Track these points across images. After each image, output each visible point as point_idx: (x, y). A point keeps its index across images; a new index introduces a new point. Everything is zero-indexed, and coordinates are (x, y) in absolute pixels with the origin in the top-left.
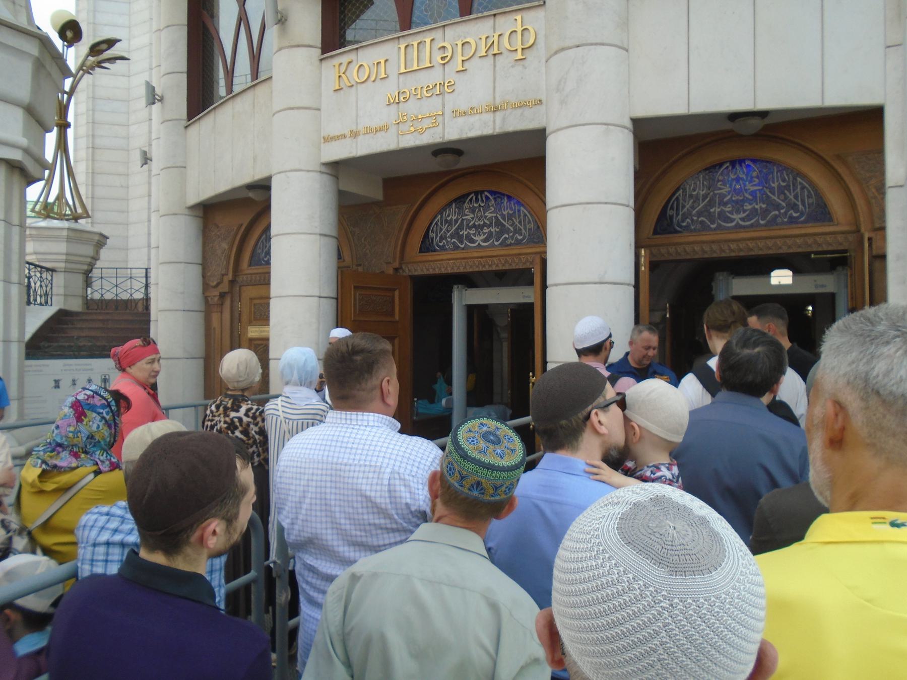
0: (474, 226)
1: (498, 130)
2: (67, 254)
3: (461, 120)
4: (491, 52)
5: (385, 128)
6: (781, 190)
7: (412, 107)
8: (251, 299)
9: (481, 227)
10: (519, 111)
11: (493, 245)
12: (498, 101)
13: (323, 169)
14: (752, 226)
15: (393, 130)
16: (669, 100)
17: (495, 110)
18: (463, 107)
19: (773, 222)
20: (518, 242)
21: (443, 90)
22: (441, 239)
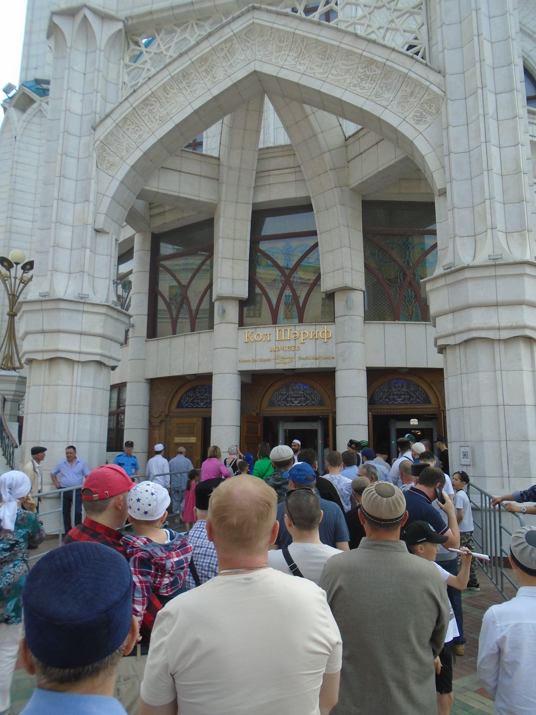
0: (294, 397)
1: (317, 367)
2: (15, 391)
3: (302, 361)
4: (314, 338)
5: (269, 360)
6: (414, 392)
7: (281, 354)
8: (177, 424)
9: (297, 397)
10: (326, 360)
11: (302, 405)
12: (317, 356)
13: (238, 373)
14: (404, 404)
15: (273, 361)
16: (379, 363)
17: (316, 359)
18: (303, 356)
19: (411, 403)
20: (313, 405)
21: (295, 349)
22: (279, 401)
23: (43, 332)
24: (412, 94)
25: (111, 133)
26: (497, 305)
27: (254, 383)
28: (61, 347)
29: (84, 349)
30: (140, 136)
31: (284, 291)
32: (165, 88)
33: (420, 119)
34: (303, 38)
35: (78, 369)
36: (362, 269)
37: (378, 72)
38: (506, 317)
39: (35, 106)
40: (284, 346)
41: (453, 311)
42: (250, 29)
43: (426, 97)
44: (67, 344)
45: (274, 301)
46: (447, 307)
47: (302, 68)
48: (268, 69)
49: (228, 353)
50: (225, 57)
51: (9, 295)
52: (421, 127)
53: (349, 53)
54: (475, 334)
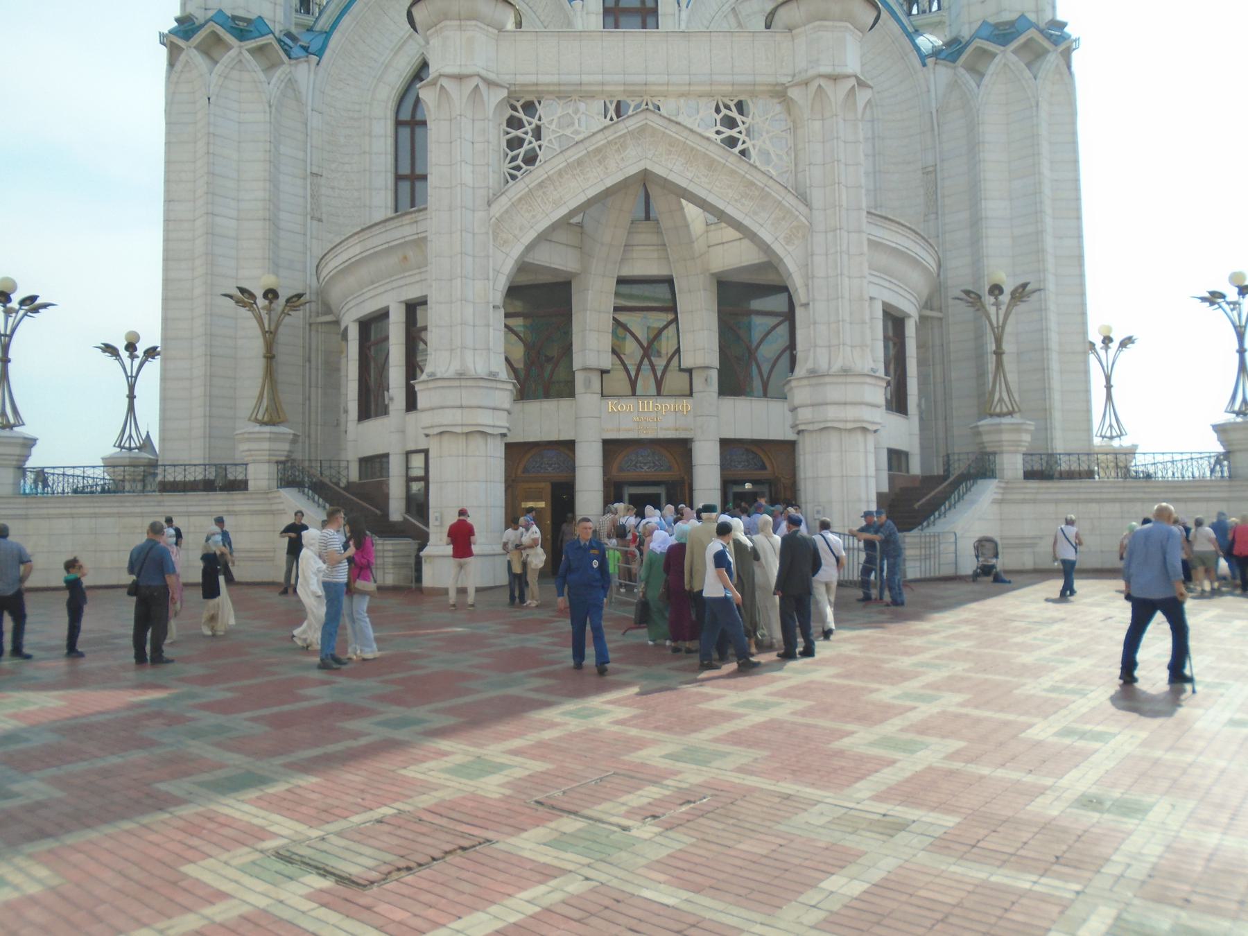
23: (461, 407)
24: (784, 218)
25: (507, 211)
26: (845, 404)
28: (480, 421)
29: (498, 423)
30: (534, 217)
31: (648, 366)
32: (560, 173)
33: (789, 240)
34: (692, 149)
35: (490, 440)
36: (717, 349)
37: (757, 193)
38: (851, 413)
39: (233, 53)
41: (813, 405)
42: (642, 130)
43: (795, 223)
44: (485, 419)
45: (633, 374)
46: (809, 402)
47: (690, 175)
48: (658, 170)
50: (618, 150)
51: (264, 333)
52: (790, 248)
53: (733, 172)
54: (829, 425)
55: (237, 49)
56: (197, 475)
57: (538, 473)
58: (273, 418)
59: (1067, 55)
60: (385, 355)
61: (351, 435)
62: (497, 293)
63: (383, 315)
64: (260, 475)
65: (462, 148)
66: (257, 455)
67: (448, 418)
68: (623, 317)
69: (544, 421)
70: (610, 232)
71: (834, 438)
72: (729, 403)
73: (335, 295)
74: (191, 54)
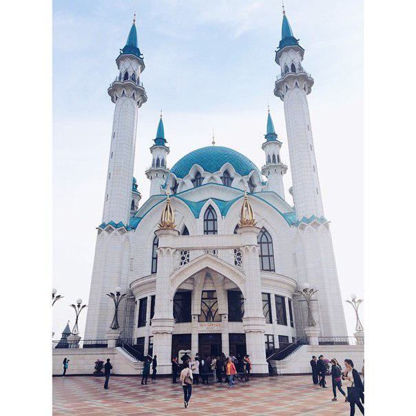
27: (202, 337)
40: (207, 328)
44: (167, 329)
49: (195, 328)
55: (116, 231)
56: (94, 343)
57: (181, 342)
58: (116, 327)
59: (327, 226)
60: (144, 310)
61: (135, 331)
62: (174, 290)
63: (147, 298)
64: (111, 343)
65: (168, 263)
66: (111, 338)
67: (159, 329)
68: (204, 301)
69: (183, 329)
70: (200, 280)
71: (253, 334)
72: (231, 323)
73: (134, 292)
74: (104, 232)
